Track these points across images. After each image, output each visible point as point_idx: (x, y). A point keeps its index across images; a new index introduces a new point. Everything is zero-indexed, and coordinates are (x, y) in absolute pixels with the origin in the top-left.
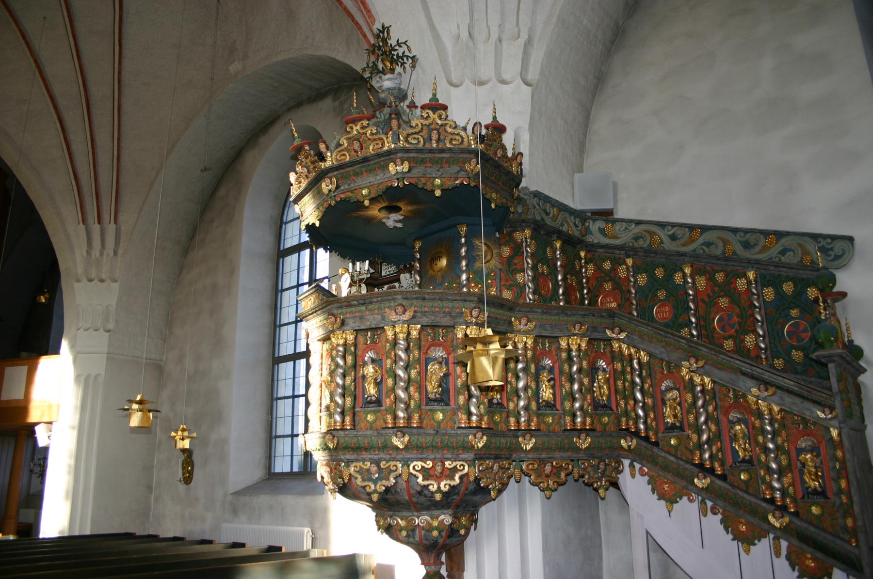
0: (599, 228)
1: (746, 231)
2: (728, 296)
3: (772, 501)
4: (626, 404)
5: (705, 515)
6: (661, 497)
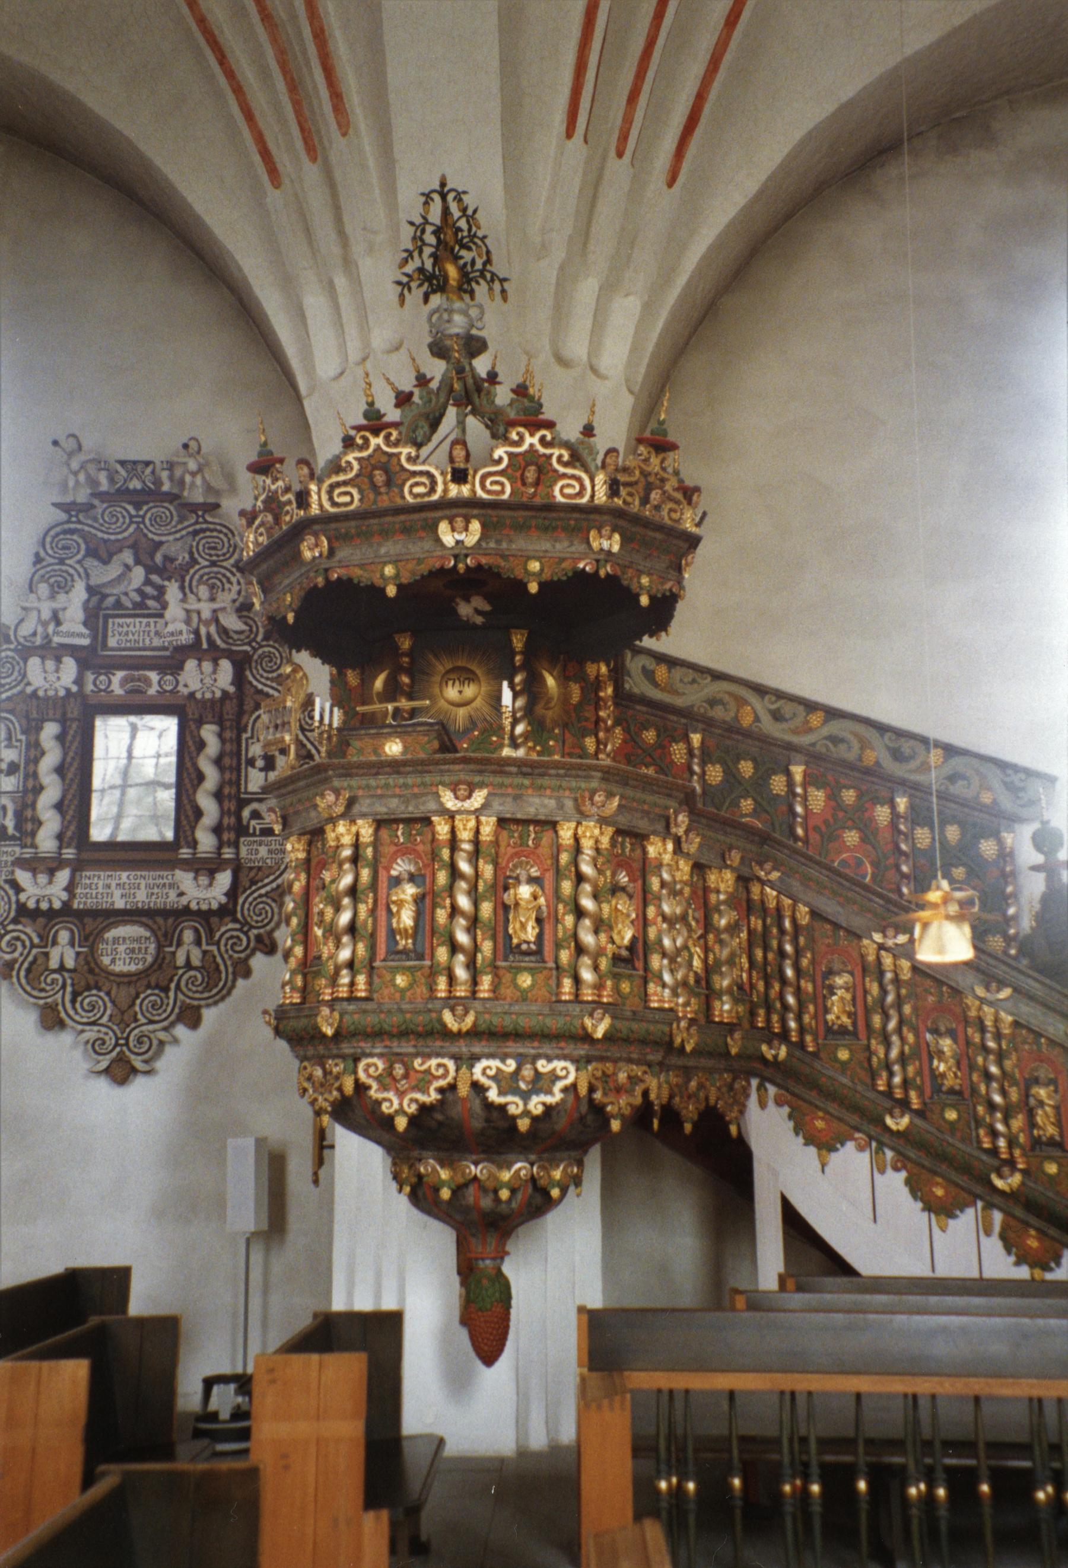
0: (644, 668)
1: (900, 734)
2: (859, 829)
3: (994, 1151)
4: (768, 986)
5: (882, 1171)
6: (809, 1141)
